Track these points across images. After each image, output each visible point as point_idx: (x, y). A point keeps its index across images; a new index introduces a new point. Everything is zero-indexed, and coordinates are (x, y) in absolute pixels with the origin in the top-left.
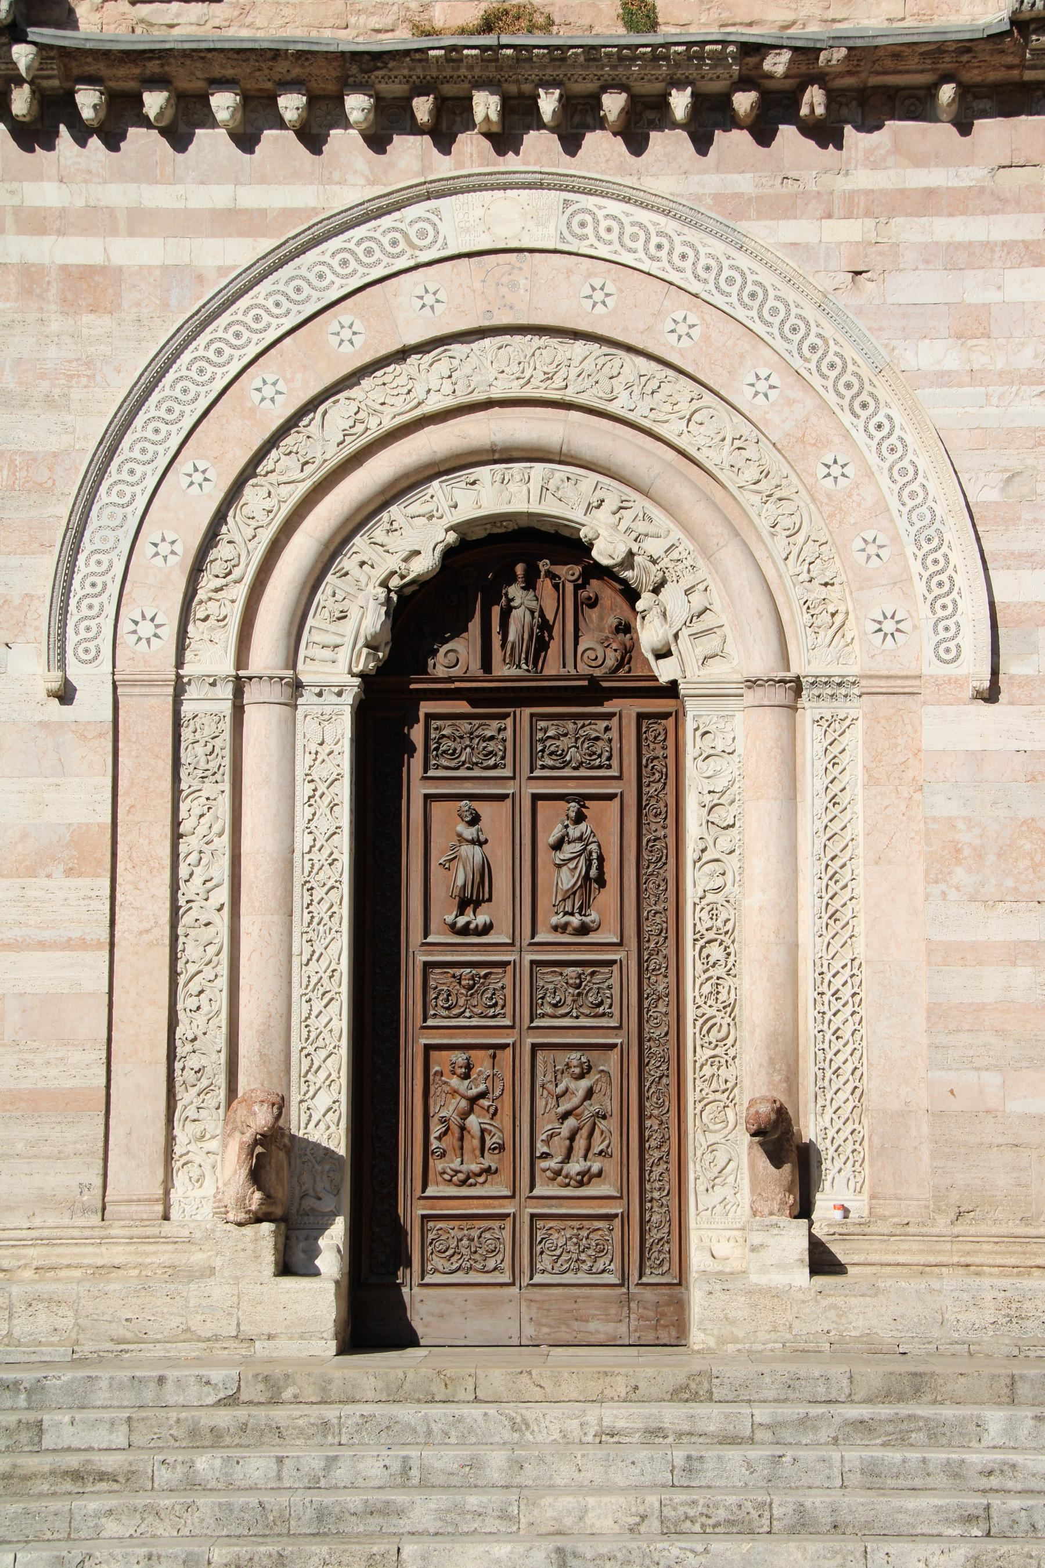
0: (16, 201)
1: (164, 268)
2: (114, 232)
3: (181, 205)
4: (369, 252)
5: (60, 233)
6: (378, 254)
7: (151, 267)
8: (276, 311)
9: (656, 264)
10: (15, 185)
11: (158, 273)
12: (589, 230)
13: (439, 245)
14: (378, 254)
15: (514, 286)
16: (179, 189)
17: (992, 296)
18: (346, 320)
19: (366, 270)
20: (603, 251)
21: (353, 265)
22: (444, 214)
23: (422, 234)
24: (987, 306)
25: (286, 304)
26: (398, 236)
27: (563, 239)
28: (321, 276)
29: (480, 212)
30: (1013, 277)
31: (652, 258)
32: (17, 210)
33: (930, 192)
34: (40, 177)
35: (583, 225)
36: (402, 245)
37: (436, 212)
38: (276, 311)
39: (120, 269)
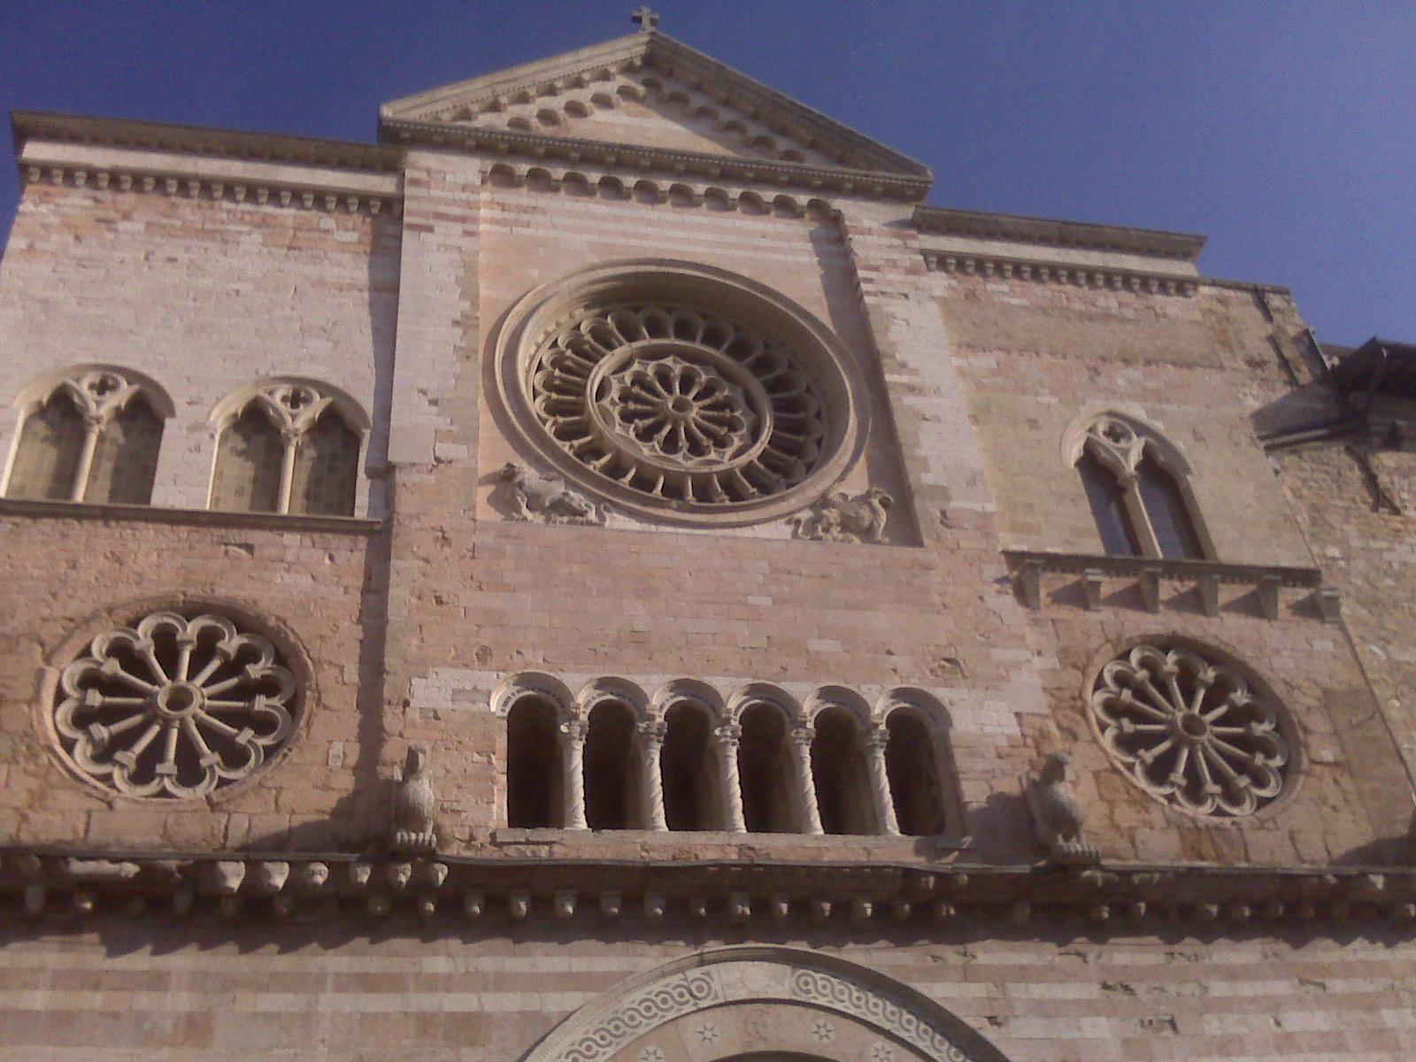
0: (416, 969)
1: (521, 1013)
2: (485, 989)
3: (533, 970)
4: (664, 1001)
5: (447, 990)
6: (671, 1003)
7: (513, 1013)
8: (602, 1043)
9: (859, 1010)
10: (415, 960)
11: (517, 1017)
12: (811, 987)
13: (711, 997)
14: (671, 1003)
15: (765, 1025)
16: (531, 960)
17: (1077, 1035)
18: (651, 1049)
19: (663, 1013)
20: (822, 1001)
21: (654, 1010)
22: (715, 976)
23: (700, 989)
24: (1074, 1041)
25: (609, 1038)
26: (684, 990)
27: (795, 993)
28: (632, 1018)
29: (738, 975)
30: (1086, 1022)
31: (856, 1006)
32: (417, 975)
33: (1022, 967)
34: (435, 953)
35: (807, 984)
36: (687, 996)
37: (708, 974)
38: (602, 1043)
39: (490, 1015)
